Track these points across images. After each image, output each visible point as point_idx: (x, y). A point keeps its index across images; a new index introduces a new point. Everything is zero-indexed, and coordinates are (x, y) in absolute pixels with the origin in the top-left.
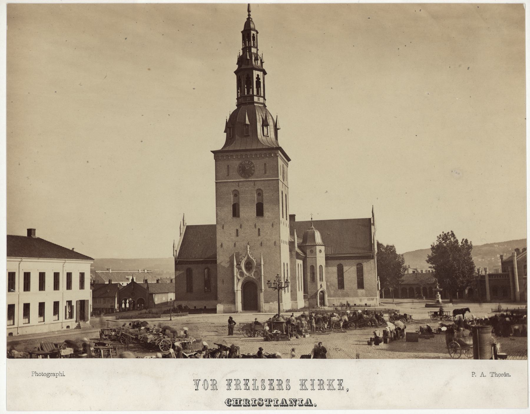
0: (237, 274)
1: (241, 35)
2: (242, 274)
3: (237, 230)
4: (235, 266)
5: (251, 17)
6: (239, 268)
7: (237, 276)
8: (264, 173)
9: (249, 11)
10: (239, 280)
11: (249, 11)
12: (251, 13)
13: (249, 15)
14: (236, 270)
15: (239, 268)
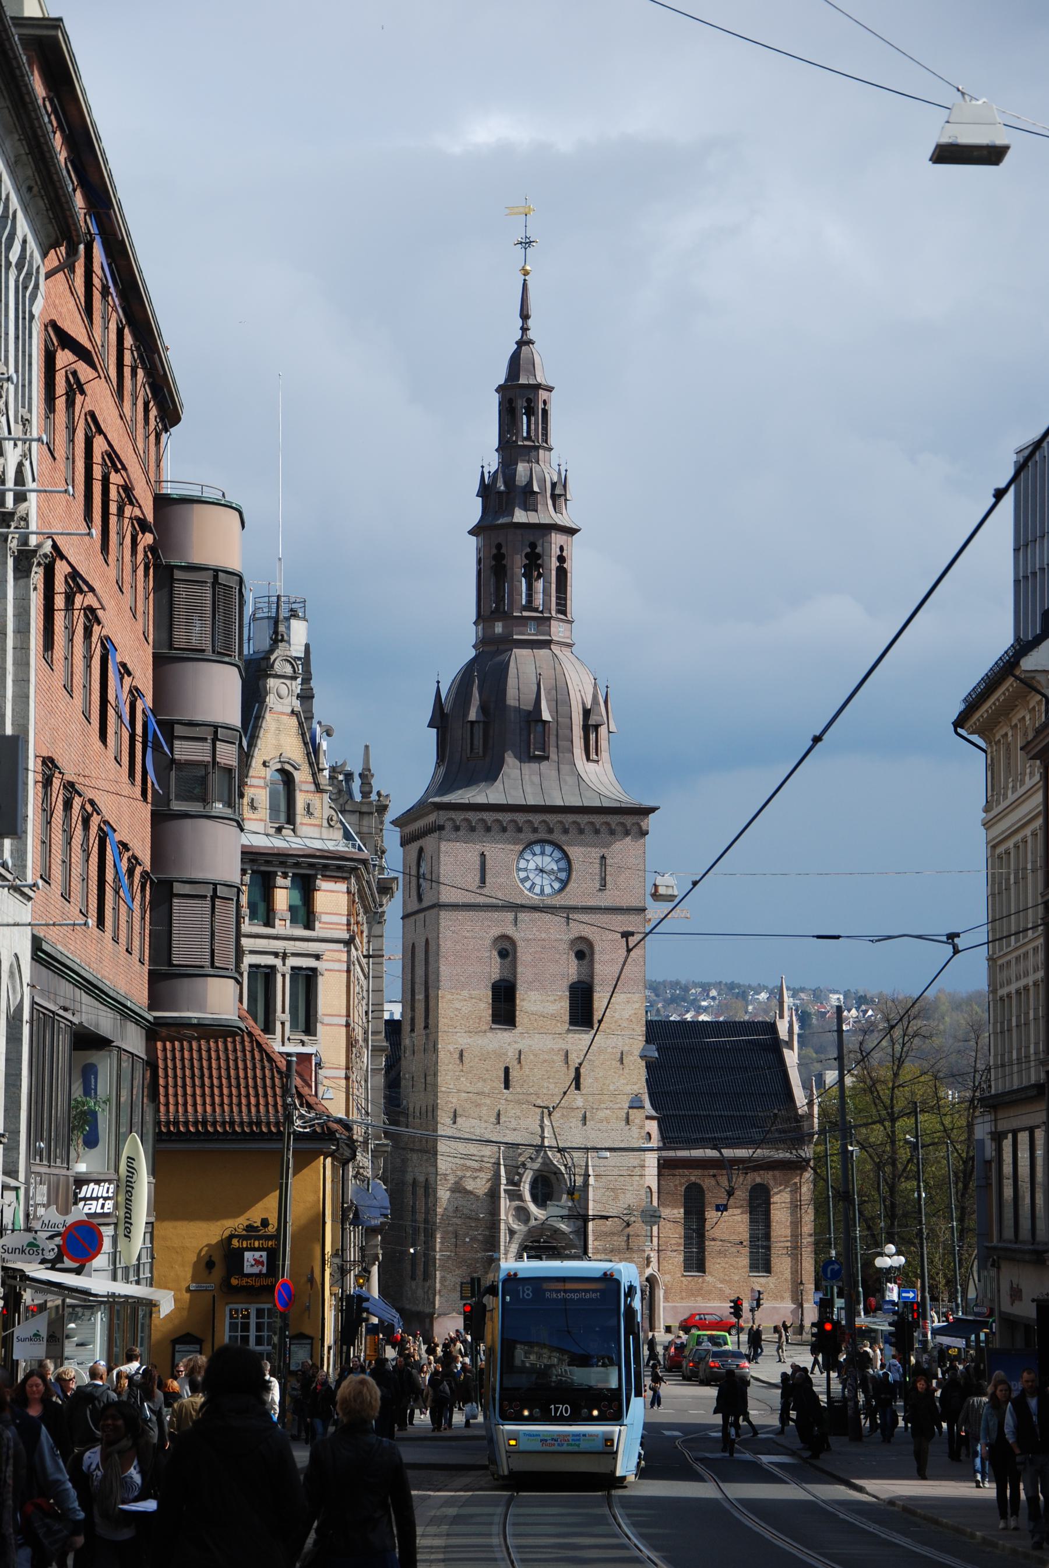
0: (507, 1216)
1: (495, 398)
2: (522, 1214)
3: (507, 1070)
4: (503, 1187)
5: (531, 335)
6: (515, 1195)
7: (507, 1223)
8: (598, 886)
9: (525, 316)
10: (512, 1232)
11: (525, 316)
12: (530, 323)
13: (524, 329)
14: (504, 1203)
15: (515, 1195)
